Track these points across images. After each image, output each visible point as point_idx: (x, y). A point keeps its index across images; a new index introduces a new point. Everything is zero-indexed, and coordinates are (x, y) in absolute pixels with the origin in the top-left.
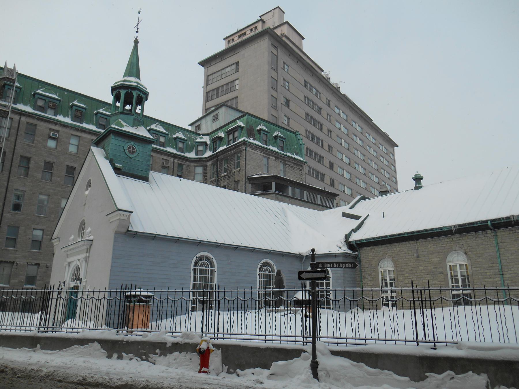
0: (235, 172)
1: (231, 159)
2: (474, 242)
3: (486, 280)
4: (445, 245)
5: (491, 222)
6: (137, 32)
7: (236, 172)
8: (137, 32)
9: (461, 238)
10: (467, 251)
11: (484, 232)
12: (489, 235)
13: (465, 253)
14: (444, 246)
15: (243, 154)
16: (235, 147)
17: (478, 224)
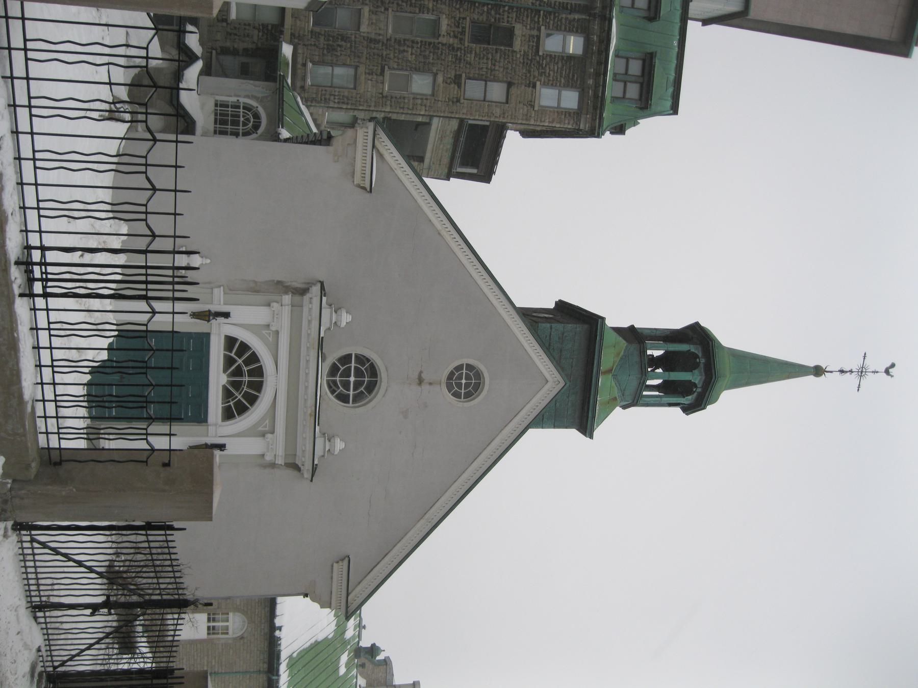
0: (534, 86)
1: (573, 76)
2: (256, 649)
3: (206, 658)
4: (257, 613)
5: (276, 679)
7: (532, 91)
9: (262, 634)
10: (245, 641)
11: (266, 660)
12: (261, 665)
13: (242, 638)
14: (255, 612)
15: (569, 123)
16: (598, 96)
17: (277, 665)
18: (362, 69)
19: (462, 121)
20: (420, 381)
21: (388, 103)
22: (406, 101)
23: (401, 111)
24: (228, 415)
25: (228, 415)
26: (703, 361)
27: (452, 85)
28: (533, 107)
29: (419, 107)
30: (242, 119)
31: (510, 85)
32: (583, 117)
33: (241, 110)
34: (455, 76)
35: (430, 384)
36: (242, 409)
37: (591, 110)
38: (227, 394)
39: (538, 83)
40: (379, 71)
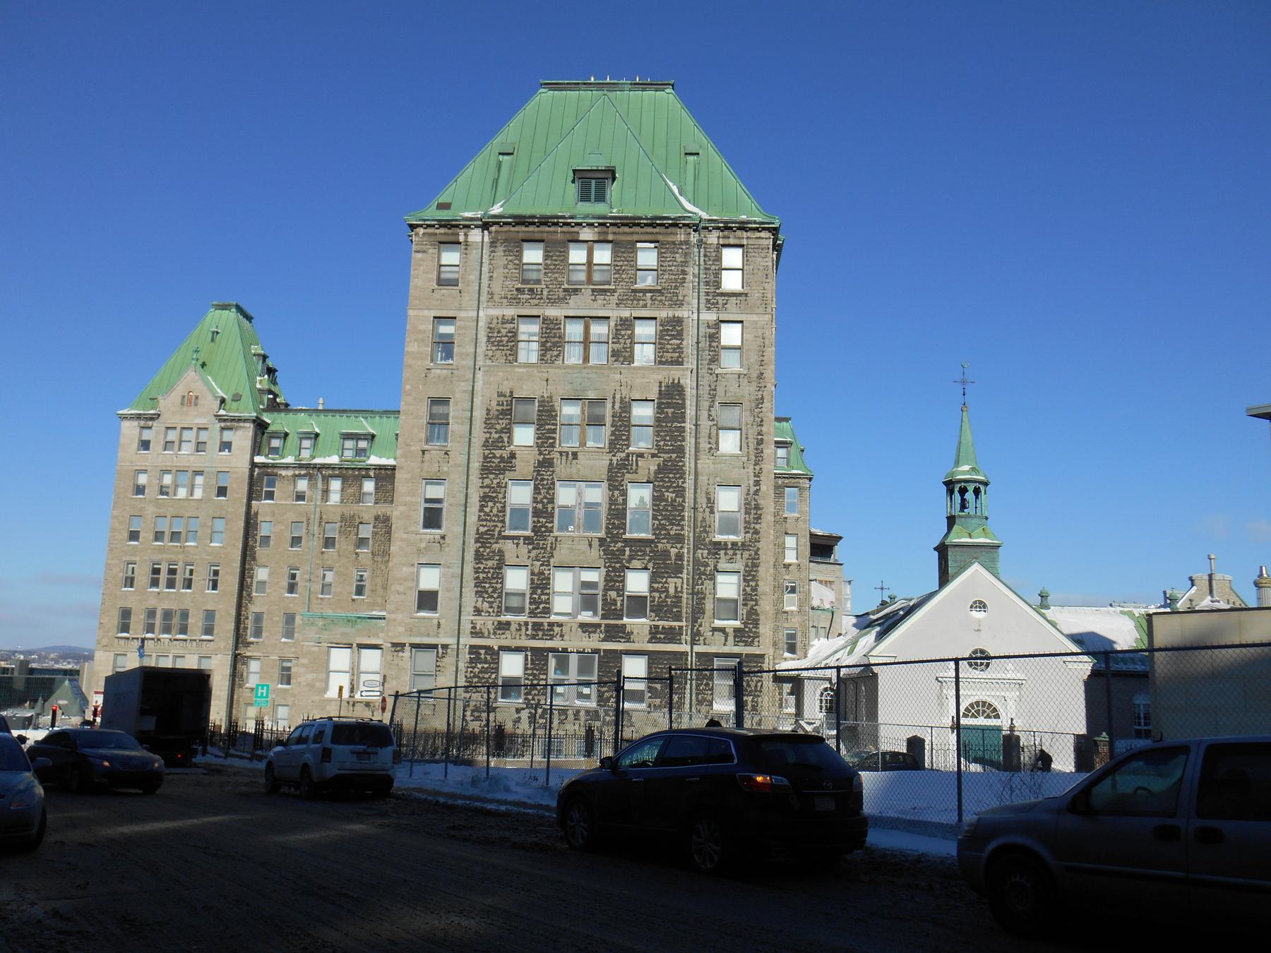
0: (786, 518)
6: (964, 395)
8: (964, 395)
18: (786, 625)
19: (810, 561)
20: (979, 630)
21: (804, 608)
22: (801, 597)
23: (808, 600)
24: (997, 717)
25: (997, 717)
26: (963, 484)
27: (790, 569)
28: (798, 518)
29: (805, 589)
30: (829, 698)
31: (786, 533)
32: (801, 485)
33: (823, 698)
34: (784, 568)
35: (980, 625)
36: (995, 710)
37: (797, 480)
38: (988, 717)
39: (784, 516)
40: (786, 615)
